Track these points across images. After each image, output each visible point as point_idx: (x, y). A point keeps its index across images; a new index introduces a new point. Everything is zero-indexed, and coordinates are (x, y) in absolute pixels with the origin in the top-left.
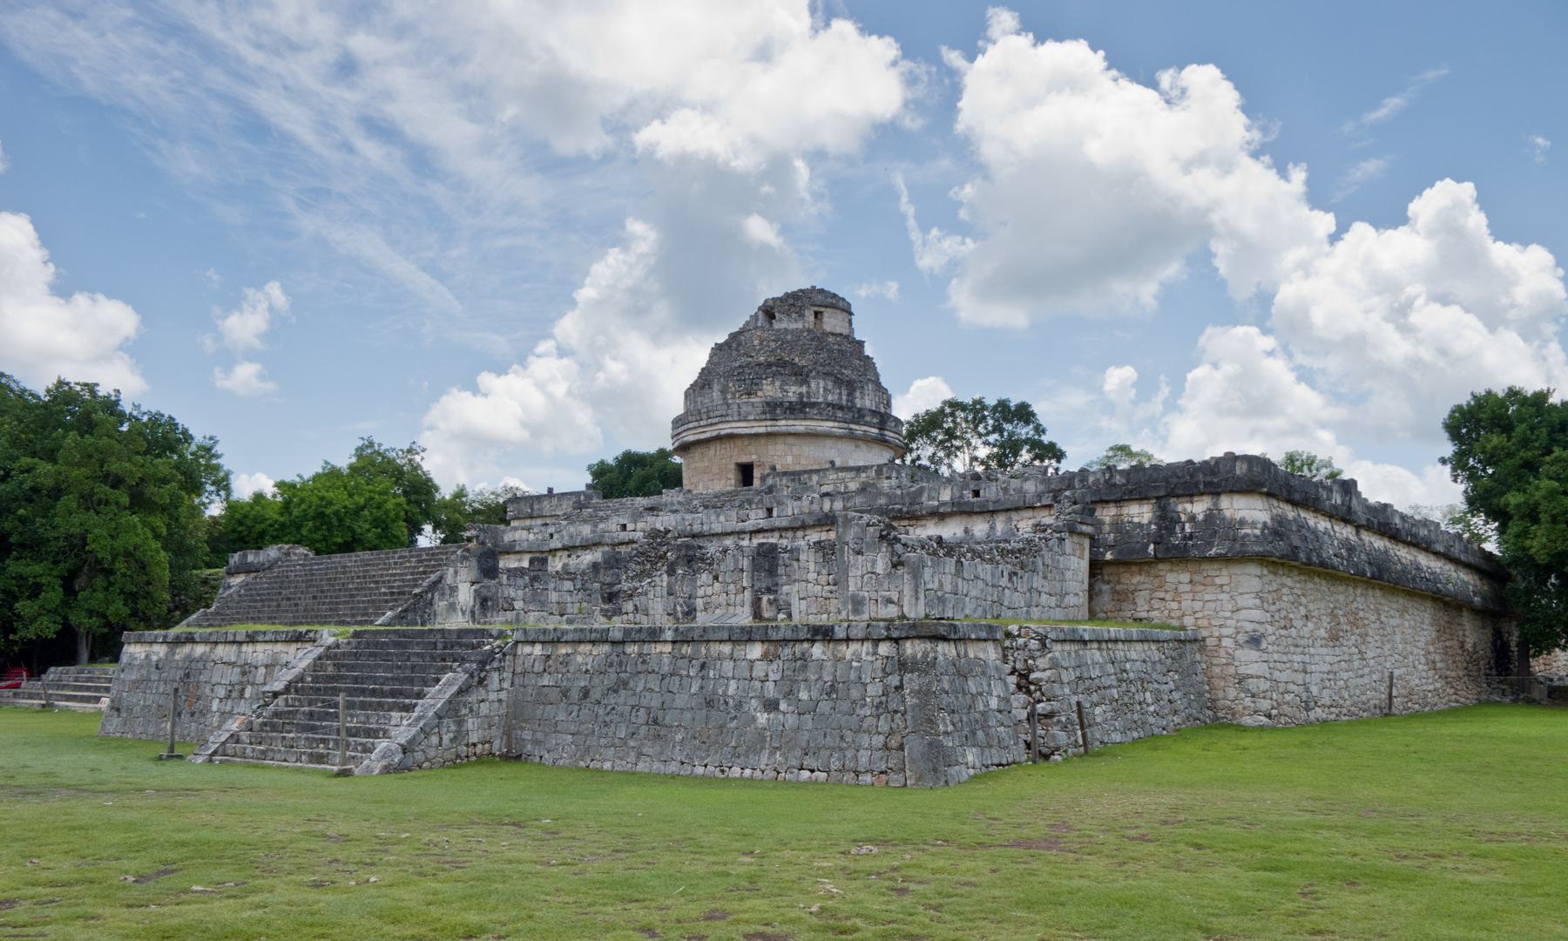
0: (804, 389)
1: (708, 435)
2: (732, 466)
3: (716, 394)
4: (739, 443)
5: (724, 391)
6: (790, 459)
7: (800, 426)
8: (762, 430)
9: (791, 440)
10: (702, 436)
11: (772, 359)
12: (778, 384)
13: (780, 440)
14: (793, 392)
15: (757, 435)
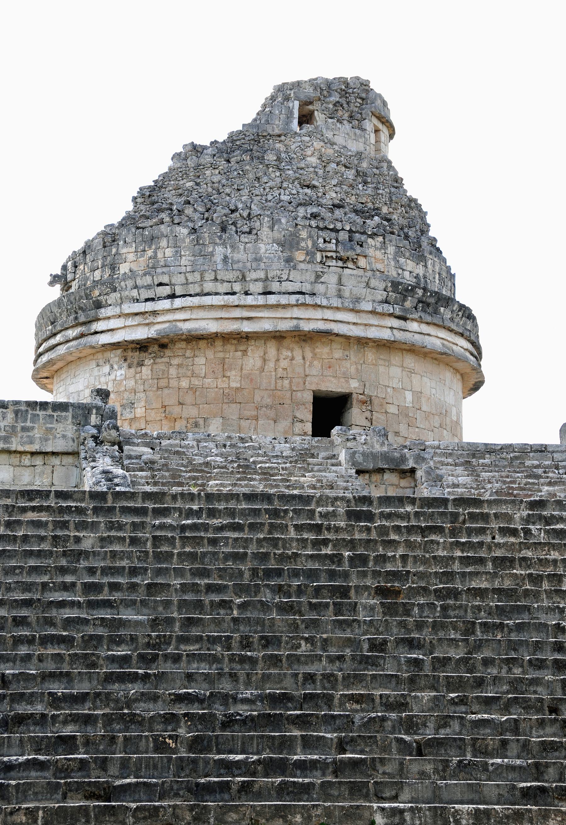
0: (420, 270)
1: (267, 326)
2: (309, 398)
3: (267, 247)
4: (323, 350)
5: (289, 243)
6: (409, 396)
7: (436, 338)
8: (386, 335)
9: (410, 361)
10: (247, 327)
11: (352, 200)
12: (391, 249)
13: (396, 359)
14: (410, 271)
15: (362, 342)
